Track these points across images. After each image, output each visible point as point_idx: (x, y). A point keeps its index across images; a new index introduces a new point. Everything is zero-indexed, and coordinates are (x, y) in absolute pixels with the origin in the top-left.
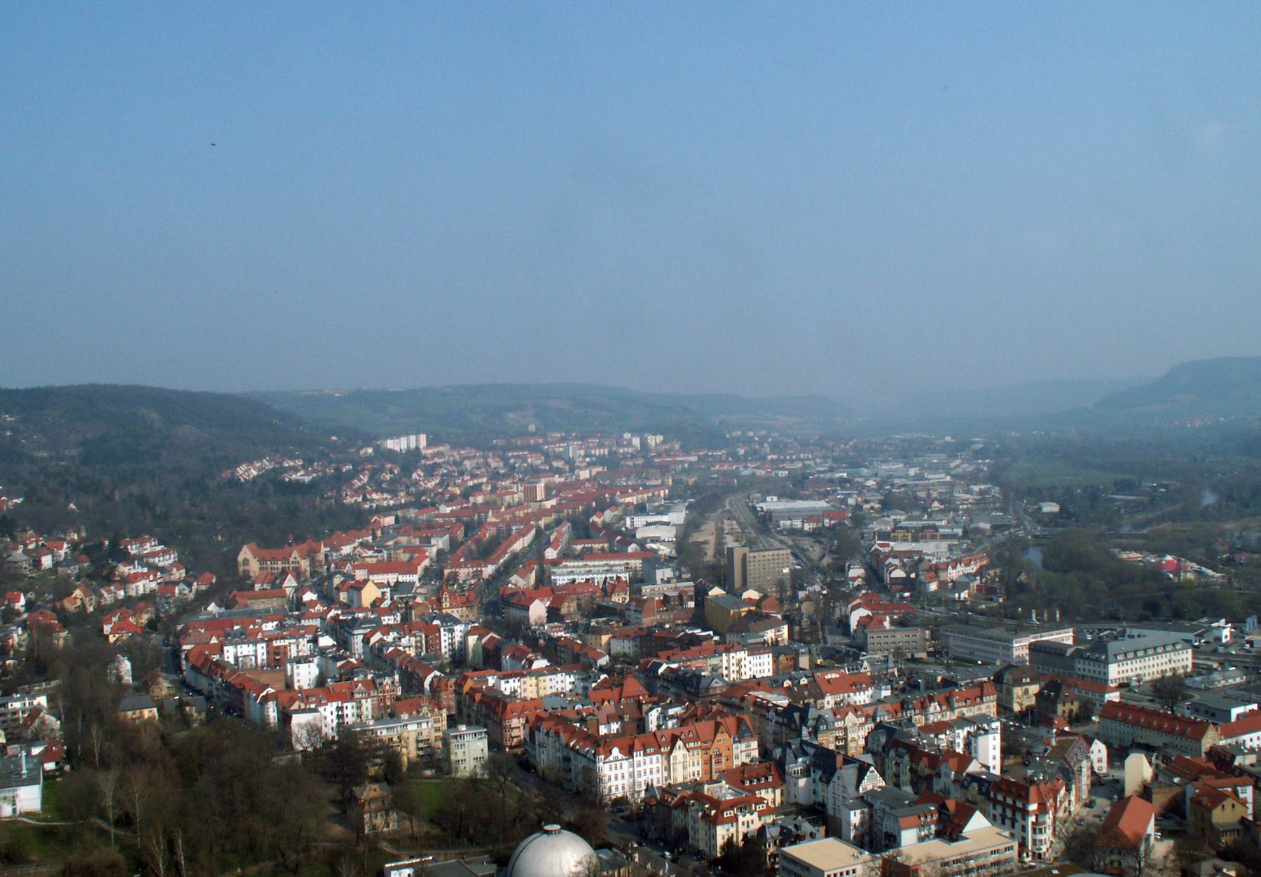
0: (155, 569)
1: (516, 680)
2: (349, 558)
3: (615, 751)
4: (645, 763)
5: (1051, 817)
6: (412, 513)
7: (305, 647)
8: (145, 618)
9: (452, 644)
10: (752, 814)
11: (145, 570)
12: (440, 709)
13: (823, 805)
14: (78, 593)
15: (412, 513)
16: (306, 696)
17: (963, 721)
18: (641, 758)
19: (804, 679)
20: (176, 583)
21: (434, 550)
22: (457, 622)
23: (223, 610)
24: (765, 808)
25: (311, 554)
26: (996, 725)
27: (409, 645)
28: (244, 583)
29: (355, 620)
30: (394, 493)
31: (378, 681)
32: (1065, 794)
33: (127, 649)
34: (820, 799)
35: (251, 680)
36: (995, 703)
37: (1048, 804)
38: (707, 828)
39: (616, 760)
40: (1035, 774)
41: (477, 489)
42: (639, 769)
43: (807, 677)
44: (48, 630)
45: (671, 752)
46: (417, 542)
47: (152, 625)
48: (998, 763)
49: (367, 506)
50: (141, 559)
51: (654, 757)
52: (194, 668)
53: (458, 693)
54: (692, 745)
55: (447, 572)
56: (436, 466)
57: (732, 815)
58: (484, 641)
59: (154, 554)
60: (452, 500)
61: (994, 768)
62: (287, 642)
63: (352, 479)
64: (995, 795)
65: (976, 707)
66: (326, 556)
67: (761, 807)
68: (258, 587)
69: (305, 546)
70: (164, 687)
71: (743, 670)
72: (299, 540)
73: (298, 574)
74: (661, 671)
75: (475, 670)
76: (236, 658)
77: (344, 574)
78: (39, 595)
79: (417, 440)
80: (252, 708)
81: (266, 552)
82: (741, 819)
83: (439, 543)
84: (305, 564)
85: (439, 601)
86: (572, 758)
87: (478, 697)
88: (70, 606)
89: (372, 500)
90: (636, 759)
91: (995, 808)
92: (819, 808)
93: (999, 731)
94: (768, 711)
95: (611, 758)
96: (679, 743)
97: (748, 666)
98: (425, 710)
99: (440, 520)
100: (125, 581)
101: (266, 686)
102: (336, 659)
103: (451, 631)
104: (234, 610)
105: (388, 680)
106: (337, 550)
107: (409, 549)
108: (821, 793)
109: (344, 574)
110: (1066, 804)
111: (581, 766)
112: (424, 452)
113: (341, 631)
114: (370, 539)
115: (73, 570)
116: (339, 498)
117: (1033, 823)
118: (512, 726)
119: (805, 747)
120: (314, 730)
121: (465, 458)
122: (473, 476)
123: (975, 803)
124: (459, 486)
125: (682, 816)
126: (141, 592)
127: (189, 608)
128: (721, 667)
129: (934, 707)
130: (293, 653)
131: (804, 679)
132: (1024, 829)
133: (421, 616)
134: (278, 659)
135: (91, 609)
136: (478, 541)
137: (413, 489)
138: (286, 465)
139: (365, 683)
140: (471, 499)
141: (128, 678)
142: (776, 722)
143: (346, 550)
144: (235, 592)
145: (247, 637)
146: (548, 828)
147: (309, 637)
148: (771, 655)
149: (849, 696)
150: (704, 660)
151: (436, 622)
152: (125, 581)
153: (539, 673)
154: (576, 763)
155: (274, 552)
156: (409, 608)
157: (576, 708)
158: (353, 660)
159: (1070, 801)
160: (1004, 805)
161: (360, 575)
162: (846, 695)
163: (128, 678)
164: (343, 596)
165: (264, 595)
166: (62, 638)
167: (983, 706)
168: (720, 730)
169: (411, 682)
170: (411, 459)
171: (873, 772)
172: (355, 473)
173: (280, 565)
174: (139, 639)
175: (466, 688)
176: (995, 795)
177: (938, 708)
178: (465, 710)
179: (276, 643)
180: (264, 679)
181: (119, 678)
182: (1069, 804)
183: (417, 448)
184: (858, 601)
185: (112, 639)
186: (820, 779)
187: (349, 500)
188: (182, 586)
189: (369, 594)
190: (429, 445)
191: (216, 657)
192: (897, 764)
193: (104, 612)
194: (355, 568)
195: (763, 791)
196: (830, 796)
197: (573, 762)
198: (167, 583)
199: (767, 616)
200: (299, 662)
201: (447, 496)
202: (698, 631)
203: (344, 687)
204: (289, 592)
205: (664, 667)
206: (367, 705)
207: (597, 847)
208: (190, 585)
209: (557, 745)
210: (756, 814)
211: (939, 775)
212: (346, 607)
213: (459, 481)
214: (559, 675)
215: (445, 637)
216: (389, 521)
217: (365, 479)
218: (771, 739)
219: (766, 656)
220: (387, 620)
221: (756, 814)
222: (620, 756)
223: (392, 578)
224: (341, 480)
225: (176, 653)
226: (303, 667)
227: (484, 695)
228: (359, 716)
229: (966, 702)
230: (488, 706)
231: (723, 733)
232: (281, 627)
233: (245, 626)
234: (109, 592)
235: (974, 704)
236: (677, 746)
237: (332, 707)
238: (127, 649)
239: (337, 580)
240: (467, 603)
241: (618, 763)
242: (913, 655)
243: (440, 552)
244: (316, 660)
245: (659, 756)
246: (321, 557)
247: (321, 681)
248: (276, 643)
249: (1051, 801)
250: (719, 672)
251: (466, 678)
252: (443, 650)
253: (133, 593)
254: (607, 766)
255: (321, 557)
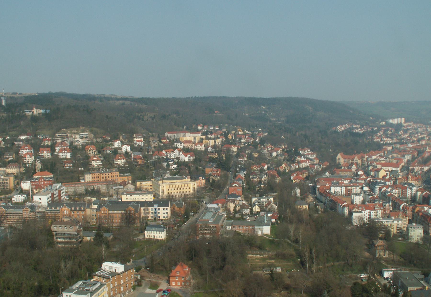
0: (308, 159)
2: (375, 160)
6: (398, 146)
7: (358, 190)
8: (305, 175)
9: (411, 194)
11: (305, 159)
12: (406, 216)
14: (283, 165)
15: (398, 146)
16: (358, 207)
20: (315, 164)
21: (406, 160)
22: (414, 186)
23: (330, 175)
25: (362, 158)
27: (396, 192)
28: (338, 166)
29: (377, 182)
30: (392, 138)
31: (384, 204)
33: (299, 185)
35: (339, 199)
41: (423, 139)
44: (274, 177)
46: (399, 156)
47: (307, 178)
49: (382, 142)
50: (304, 155)
52: (320, 193)
53: (413, 212)
55: (410, 168)
56: (408, 130)
58: (424, 194)
59: (308, 154)
60: (413, 142)
62: (352, 188)
63: (377, 133)
66: (367, 159)
68: (343, 168)
69: (360, 155)
70: (310, 199)
72: (358, 153)
73: (357, 164)
75: (419, 204)
76: (335, 191)
77: (373, 166)
78: (271, 165)
79: (401, 120)
80: (339, 209)
81: (347, 156)
83: (408, 157)
84: (359, 161)
85: (407, 178)
87: (420, 214)
88: (281, 169)
89: (384, 141)
98: (400, 216)
99: (409, 149)
100: (299, 162)
101: (345, 202)
102: (369, 195)
103: (411, 189)
104: (335, 175)
105: (387, 204)
106: (371, 157)
107: (396, 159)
109: (373, 166)
112: (403, 124)
113: (371, 185)
114: (383, 154)
115: (282, 158)
116: (372, 139)
120: (361, 219)
121: (419, 127)
122: (421, 134)
124: (416, 137)
126: (304, 166)
127: (320, 173)
130: (354, 191)
133: (400, 183)
134: (349, 193)
135: (287, 171)
136: (423, 158)
137: (399, 138)
138: (354, 127)
139: (379, 204)
140: (421, 142)
141: (298, 195)
143: (374, 157)
144: (335, 169)
145: (339, 185)
147: (360, 186)
151: (406, 186)
152: (299, 162)
155: (349, 156)
156: (396, 180)
158: (375, 196)
161: (379, 166)
163: (298, 195)
164: (372, 173)
165: (345, 171)
166: (278, 180)
169: (396, 206)
170: (399, 127)
172: (378, 131)
173: (351, 161)
174: (303, 182)
175: (416, 210)
178: (415, 218)
179: (348, 188)
180: (344, 199)
181: (296, 194)
183: (401, 123)
185: (294, 181)
187: (376, 140)
188: (317, 166)
189: (382, 173)
190: (406, 122)
191: (328, 191)
193: (291, 172)
194: (377, 164)
198: (312, 164)
200: (356, 195)
201: (411, 141)
203: (371, 205)
204: (354, 170)
206: (380, 212)
208: (320, 166)
212: (373, 177)
213: (416, 135)
215: (409, 191)
216: (390, 148)
217: (382, 133)
220: (388, 183)
223: (390, 168)
224: (373, 133)
225: (314, 188)
226: (358, 197)
227: (423, 213)
228: (376, 216)
230: (424, 218)
232: (350, 182)
233: (338, 181)
234: (294, 166)
237: (367, 212)
238: (299, 185)
239: (371, 168)
240: (418, 180)
243: (408, 161)
244: (362, 195)
246: (365, 159)
247: (363, 202)
248: (348, 188)
251: (416, 207)
252: (408, 196)
253: (301, 167)
255: (365, 159)
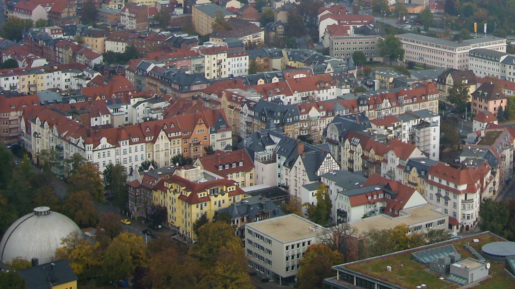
1: (16, 77)
3: (104, 141)
4: (130, 152)
5: (478, 196)
10: (223, 195)
13: (287, 188)
17: (409, 116)
18: (127, 147)
19: (275, 78)
24: (235, 189)
26: (437, 119)
32: (491, 177)
34: (283, 182)
36: (437, 101)
37: (476, 185)
38: (183, 207)
39: (104, 148)
40: (467, 160)
42: (125, 156)
43: (278, 77)
45: (153, 142)
48: (437, 150)
51: (139, 146)
54: (173, 135)
57: (206, 195)
61: (434, 155)
64: (433, 178)
65: (421, 104)
67: (233, 188)
71: (223, 70)
74: (149, 69)
82: (213, 198)
86: (64, 148)
90: (123, 147)
91: (431, 188)
92: (283, 189)
93: (439, 125)
94: (242, 106)
95: (100, 147)
96: (162, 133)
97: (228, 66)
108: (285, 177)
110: (491, 185)
111: (72, 154)
117: (462, 202)
118: (10, 119)
119: (271, 136)
123: (416, 185)
125: (162, 197)
128: (204, 67)
129: (386, 103)
131: (275, 78)
132: (455, 205)
142: (249, 115)
146: (37, 209)
148: (248, 57)
149: (313, 94)
150: (189, 61)
153: (37, 71)
154: (68, 152)
157: (70, 103)
159: (494, 183)
160: (440, 186)
162: (311, 92)
167: (427, 103)
168: (199, 122)
171: (330, 158)
176: (433, 178)
177: (389, 105)
182: (494, 185)
184: (326, 12)
186: (284, 164)
192: (351, 152)
195: (234, 175)
196: (292, 178)
197: (65, 151)
199: (247, 23)
202: (185, 36)
205: (152, 66)
207: (82, 225)
209: (51, 135)
210: (227, 194)
211: (386, 161)
214: (56, 73)
218: (245, 130)
219: (243, 58)
221: (227, 194)
222: (108, 145)
229: (413, 100)
231: (201, 124)
235: (420, 101)
236: (160, 136)
241: (106, 151)
242: (371, 59)
245: (144, 144)
249: (479, 182)
250: (202, 71)
254: (96, 153)
